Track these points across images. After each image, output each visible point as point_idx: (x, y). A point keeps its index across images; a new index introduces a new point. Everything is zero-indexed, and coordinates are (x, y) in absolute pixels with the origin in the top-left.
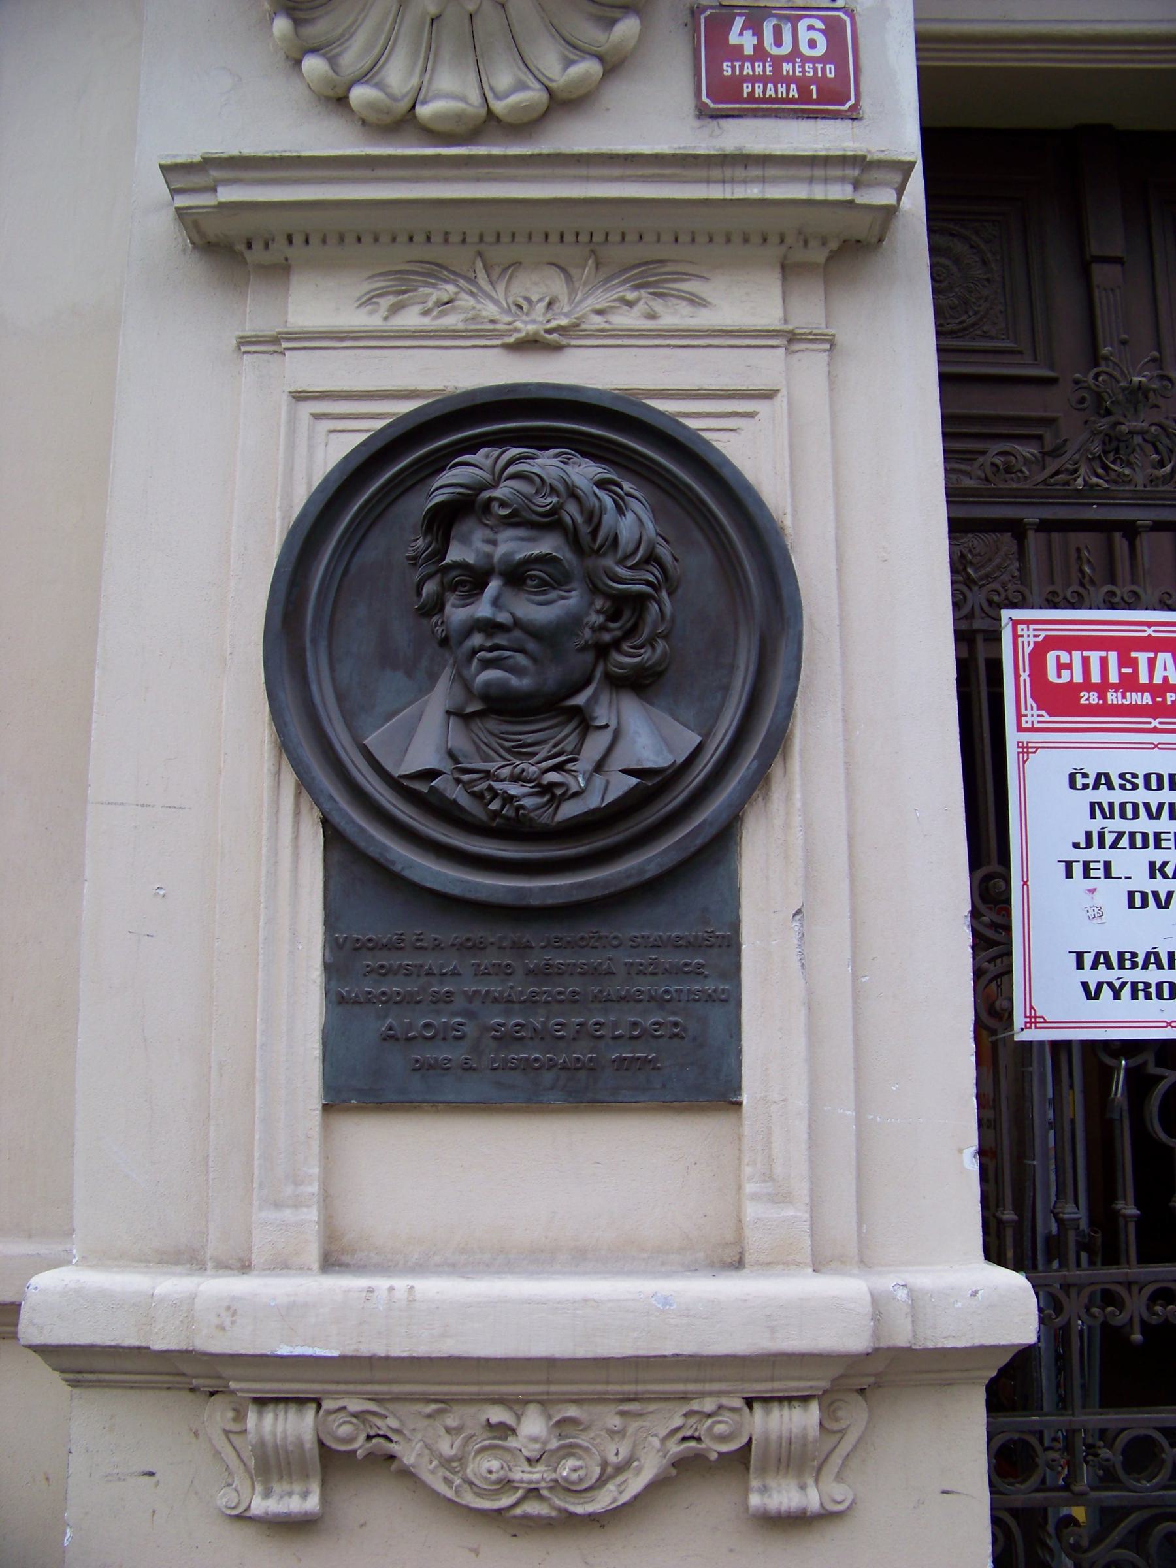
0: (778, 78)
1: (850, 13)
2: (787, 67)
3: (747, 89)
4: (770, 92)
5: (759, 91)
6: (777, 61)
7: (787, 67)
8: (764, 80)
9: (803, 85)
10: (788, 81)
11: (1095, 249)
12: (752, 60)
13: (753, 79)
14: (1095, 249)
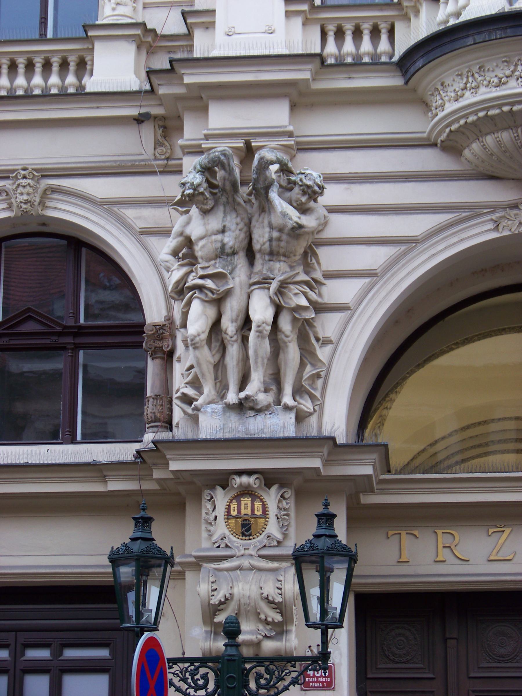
0: (318, 682)
1: (334, 665)
2: (319, 679)
3: (311, 684)
4: (316, 685)
5: (313, 685)
6: (318, 677)
7: (319, 679)
8: (315, 682)
9: (323, 683)
10: (320, 682)
11: (448, 636)
12: (312, 677)
13: (312, 682)
14: (448, 636)
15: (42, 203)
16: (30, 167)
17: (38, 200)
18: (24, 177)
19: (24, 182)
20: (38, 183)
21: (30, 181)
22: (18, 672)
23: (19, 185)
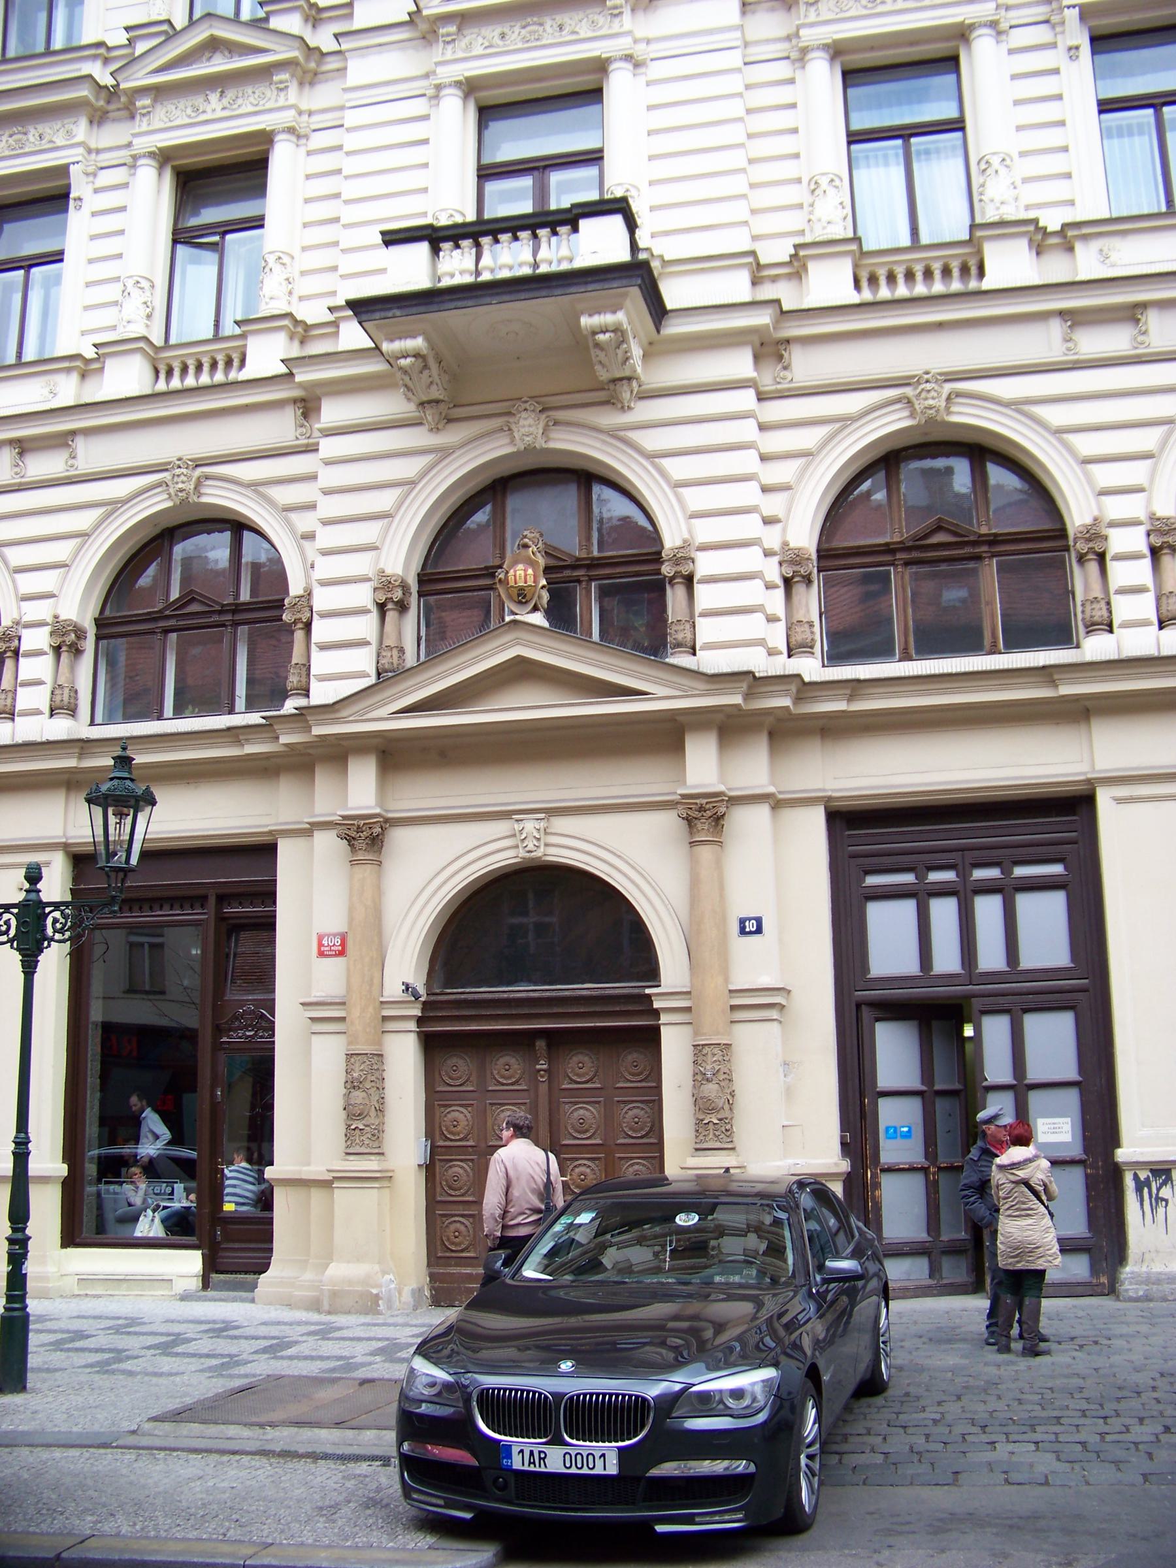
15: (947, 408)
16: (933, 371)
17: (943, 404)
18: (927, 381)
19: (928, 386)
20: (942, 387)
21: (933, 385)
22: (969, 893)
23: (923, 390)
